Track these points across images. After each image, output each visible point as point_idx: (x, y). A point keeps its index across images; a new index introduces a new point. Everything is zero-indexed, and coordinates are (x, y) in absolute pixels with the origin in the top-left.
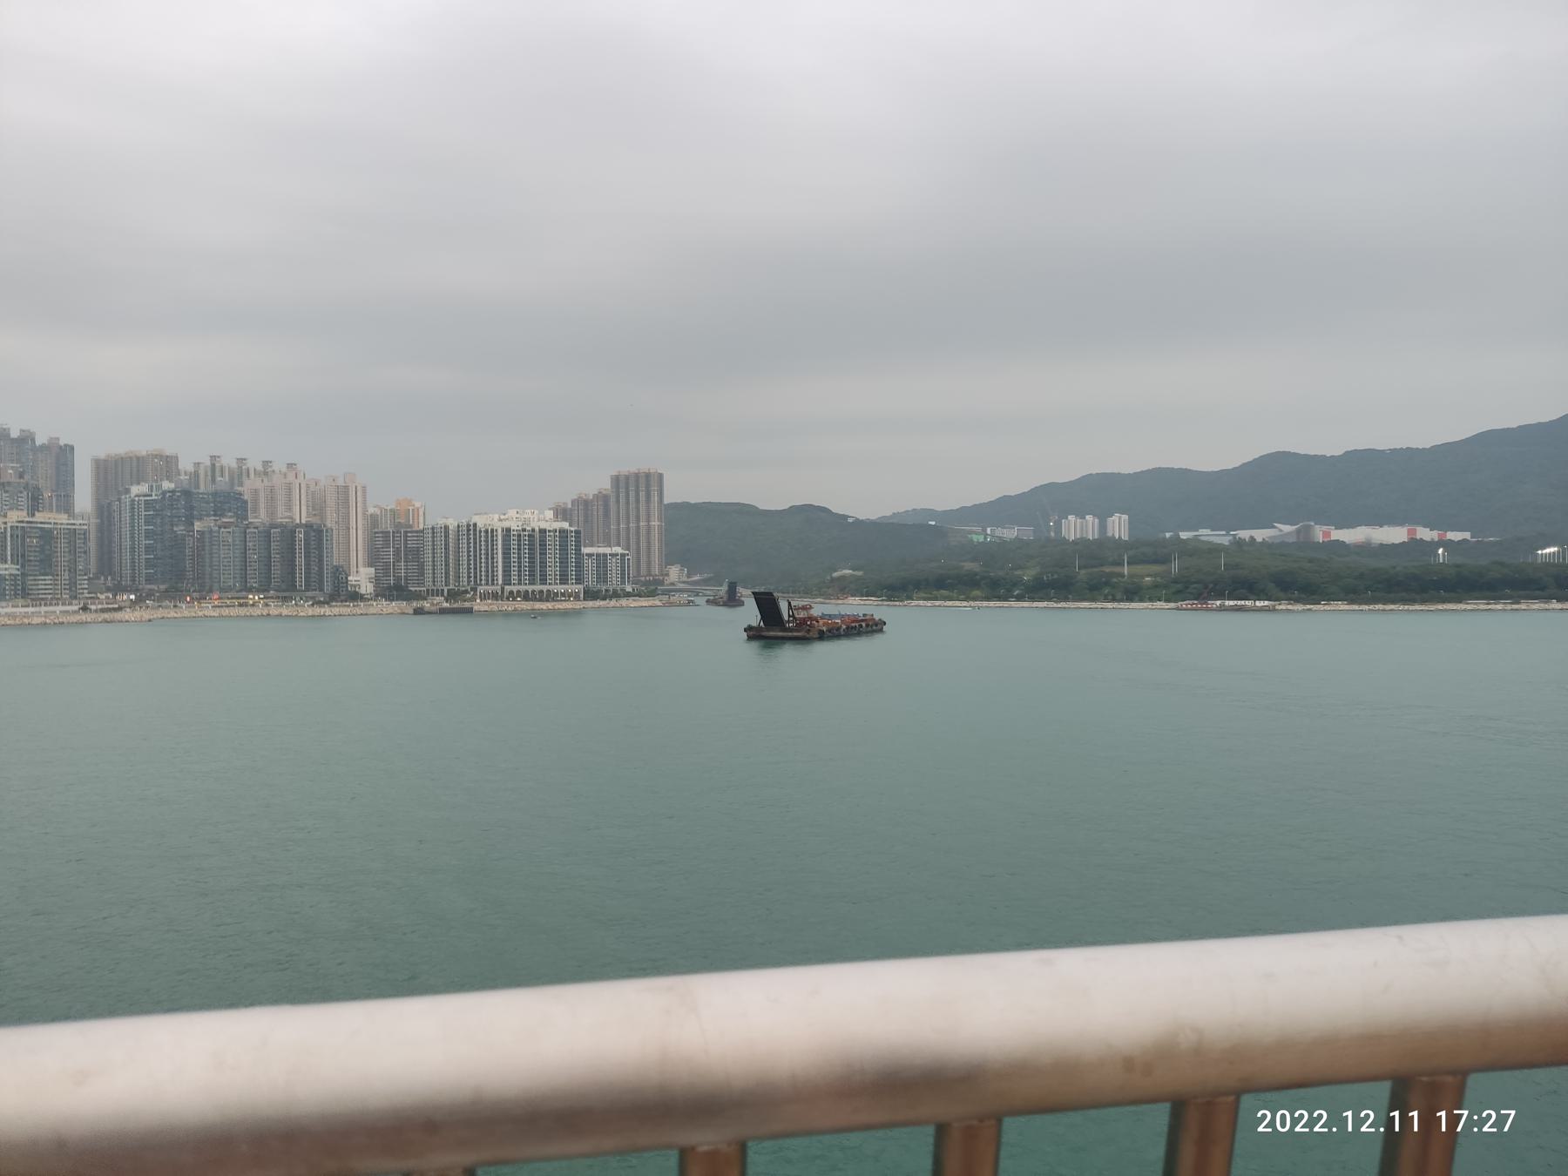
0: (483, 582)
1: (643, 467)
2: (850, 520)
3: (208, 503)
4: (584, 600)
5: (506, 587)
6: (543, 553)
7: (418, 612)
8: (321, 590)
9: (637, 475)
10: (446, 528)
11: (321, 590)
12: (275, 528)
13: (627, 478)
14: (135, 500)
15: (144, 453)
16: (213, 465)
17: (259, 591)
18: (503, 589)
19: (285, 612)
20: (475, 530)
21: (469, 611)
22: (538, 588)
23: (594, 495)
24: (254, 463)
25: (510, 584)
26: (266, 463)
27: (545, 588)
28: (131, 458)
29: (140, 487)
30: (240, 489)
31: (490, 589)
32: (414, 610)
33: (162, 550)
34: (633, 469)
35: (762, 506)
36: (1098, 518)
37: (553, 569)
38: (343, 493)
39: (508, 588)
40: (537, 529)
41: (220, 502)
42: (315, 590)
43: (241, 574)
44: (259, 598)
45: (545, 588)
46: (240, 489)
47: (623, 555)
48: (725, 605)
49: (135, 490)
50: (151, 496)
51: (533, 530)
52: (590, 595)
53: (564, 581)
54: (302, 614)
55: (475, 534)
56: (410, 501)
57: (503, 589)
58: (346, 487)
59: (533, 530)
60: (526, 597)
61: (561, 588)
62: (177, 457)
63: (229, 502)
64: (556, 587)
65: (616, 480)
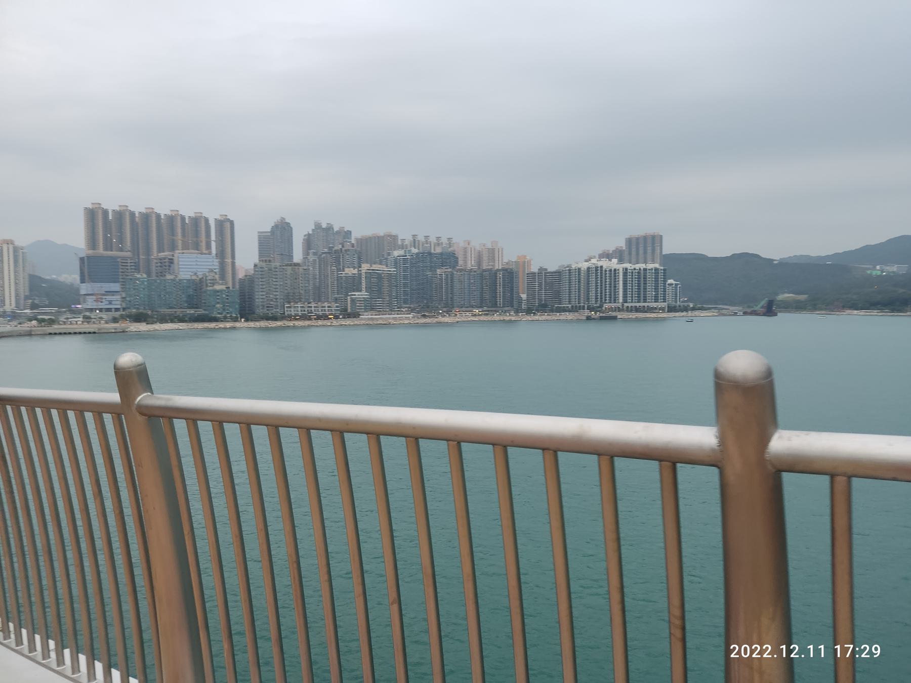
2: (775, 262)
3: (438, 259)
4: (668, 312)
5: (625, 304)
6: (645, 284)
8: (513, 306)
9: (645, 238)
11: (513, 306)
12: (485, 272)
13: (638, 239)
14: (397, 259)
15: (382, 234)
16: (414, 240)
17: (477, 307)
18: (623, 305)
19: (507, 318)
20: (601, 270)
21: (615, 318)
22: (642, 304)
23: (613, 251)
24: (433, 239)
25: (626, 302)
26: (438, 238)
27: (646, 304)
28: (375, 237)
29: (398, 251)
30: (451, 249)
31: (613, 305)
32: (587, 317)
33: (416, 286)
35: (710, 255)
37: (651, 293)
38: (492, 252)
39: (626, 305)
40: (642, 269)
41: (445, 259)
44: (479, 311)
45: (646, 304)
46: (451, 249)
47: (676, 285)
48: (764, 315)
49: (396, 253)
50: (406, 256)
51: (640, 269)
52: (671, 309)
53: (656, 301)
54: (523, 319)
55: (601, 273)
56: (525, 256)
57: (623, 305)
58: (493, 249)
59: (640, 269)
60: (637, 310)
61: (654, 305)
62: (397, 236)
63: (449, 258)
64: (652, 304)
65: (629, 241)
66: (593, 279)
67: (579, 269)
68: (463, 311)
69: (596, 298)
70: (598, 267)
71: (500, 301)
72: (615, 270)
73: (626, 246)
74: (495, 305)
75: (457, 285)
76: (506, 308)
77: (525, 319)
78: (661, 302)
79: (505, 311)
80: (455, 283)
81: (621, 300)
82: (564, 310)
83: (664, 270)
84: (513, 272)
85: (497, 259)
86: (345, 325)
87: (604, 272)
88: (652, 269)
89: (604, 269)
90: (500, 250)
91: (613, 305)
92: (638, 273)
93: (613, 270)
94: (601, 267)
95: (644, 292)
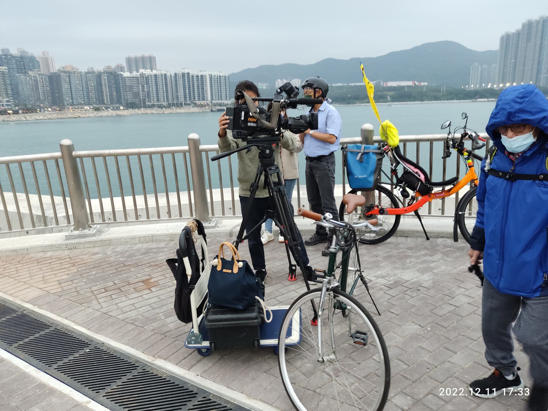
0: (196, 99)
1: (147, 54)
5: (213, 101)
6: (220, 87)
7: (212, 111)
9: (143, 58)
10: (165, 75)
12: (89, 74)
13: (136, 59)
17: (85, 104)
18: (211, 102)
31: (202, 102)
34: (139, 54)
36: (279, 79)
39: (213, 102)
42: (116, 104)
45: (222, 102)
57: (211, 102)
67: (165, 75)
68: (76, 108)
69: (185, 97)
70: (184, 74)
71: (106, 98)
72: (202, 76)
73: (126, 63)
74: (102, 102)
75: (65, 87)
76: (117, 105)
77: (168, 112)
79: (117, 108)
81: (209, 98)
84: (118, 75)
85: (52, 67)
86: (41, 120)
87: (191, 77)
89: (191, 75)
90: (53, 59)
93: (199, 76)
94: (188, 74)
95: (200, 95)
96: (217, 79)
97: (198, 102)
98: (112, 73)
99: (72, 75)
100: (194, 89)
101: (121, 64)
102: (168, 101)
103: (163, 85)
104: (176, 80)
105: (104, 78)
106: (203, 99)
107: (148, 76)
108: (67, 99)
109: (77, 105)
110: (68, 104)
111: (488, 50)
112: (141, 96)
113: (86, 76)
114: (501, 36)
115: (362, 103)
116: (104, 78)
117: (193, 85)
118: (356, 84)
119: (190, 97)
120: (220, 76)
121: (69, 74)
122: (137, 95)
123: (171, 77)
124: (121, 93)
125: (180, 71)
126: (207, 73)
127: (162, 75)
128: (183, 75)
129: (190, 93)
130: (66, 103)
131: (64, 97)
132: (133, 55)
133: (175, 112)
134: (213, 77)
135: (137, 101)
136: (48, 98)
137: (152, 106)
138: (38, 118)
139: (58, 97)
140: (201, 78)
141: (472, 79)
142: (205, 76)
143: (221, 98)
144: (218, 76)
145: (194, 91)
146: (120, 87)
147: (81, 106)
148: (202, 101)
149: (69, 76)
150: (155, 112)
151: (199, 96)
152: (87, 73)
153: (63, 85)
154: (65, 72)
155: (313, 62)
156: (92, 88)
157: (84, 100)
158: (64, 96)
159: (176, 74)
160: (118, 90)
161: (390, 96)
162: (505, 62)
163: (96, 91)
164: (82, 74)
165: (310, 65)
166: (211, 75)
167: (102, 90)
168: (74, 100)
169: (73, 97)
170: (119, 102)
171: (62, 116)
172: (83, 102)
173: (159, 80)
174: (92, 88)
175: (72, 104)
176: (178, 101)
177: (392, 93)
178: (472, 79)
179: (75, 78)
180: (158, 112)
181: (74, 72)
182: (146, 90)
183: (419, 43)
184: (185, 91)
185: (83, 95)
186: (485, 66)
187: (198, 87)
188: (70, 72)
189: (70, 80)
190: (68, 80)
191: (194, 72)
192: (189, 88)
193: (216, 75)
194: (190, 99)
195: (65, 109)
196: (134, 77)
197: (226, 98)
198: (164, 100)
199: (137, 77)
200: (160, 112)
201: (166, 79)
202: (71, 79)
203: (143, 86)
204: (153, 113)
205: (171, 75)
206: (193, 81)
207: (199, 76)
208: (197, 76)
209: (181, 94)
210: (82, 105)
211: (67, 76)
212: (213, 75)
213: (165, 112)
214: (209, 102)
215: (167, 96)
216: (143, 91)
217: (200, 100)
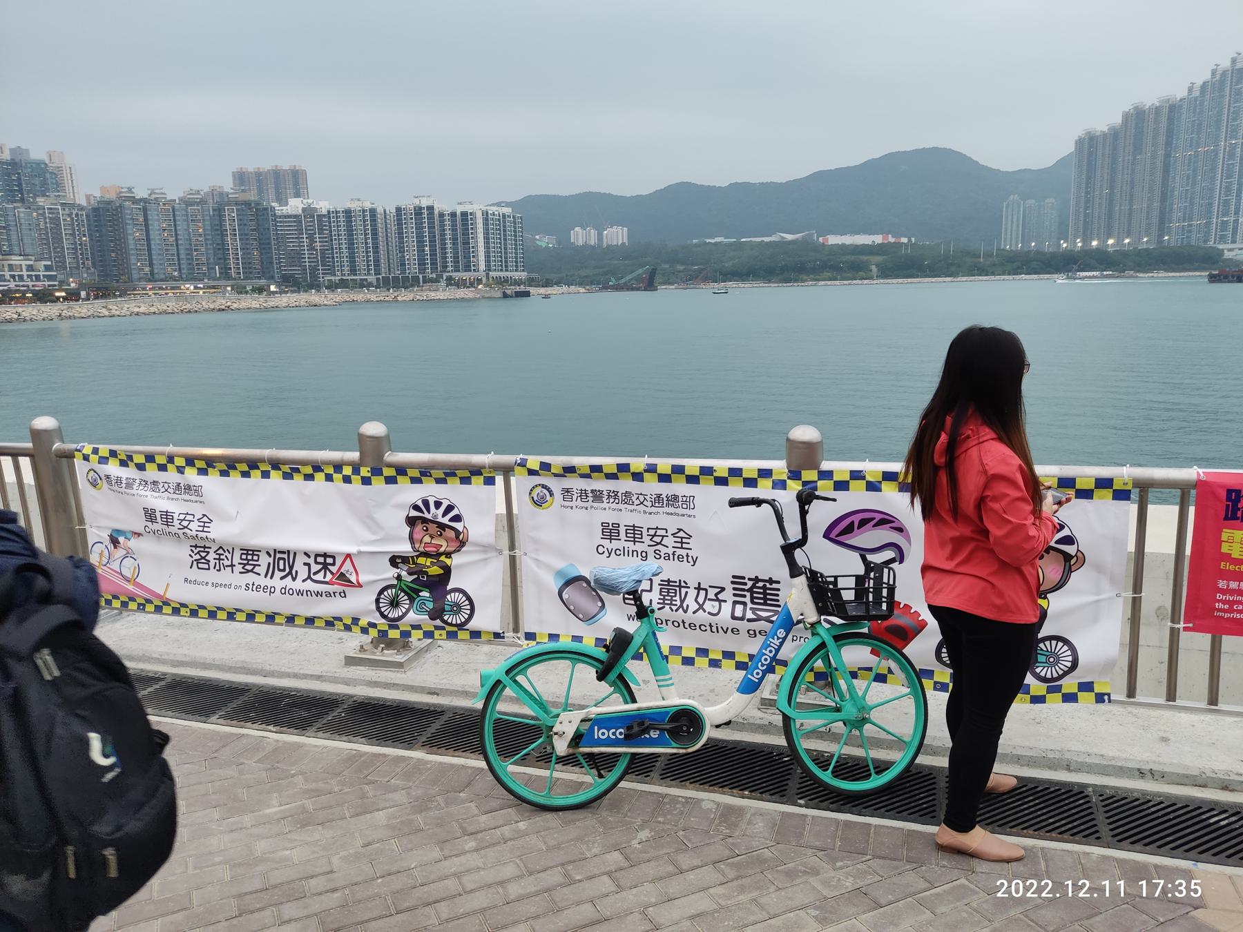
0: (450, 269)
5: (490, 273)
7: (505, 296)
11: (272, 278)
12: (192, 205)
13: (259, 175)
18: (488, 275)
25: (491, 271)
31: (465, 275)
34: (266, 166)
42: (259, 278)
43: (188, 259)
44: (196, 288)
45: (509, 274)
57: (488, 275)
59: (499, 216)
66: (410, 228)
68: (161, 288)
69: (422, 263)
70: (421, 208)
72: (464, 214)
74: (226, 274)
75: (134, 234)
76: (263, 282)
77: (404, 298)
78: (520, 271)
80: (128, 227)
81: (482, 267)
82: (363, 285)
83: (521, 218)
84: (266, 209)
86: (144, 314)
88: (509, 216)
89: (436, 212)
91: (465, 275)
92: (499, 220)
94: (430, 208)
96: (499, 220)
97: (457, 276)
98: (250, 204)
99: (152, 207)
100: (443, 244)
101: (220, 187)
102: (377, 273)
103: (366, 234)
104: (400, 224)
105: (231, 214)
106: (467, 268)
107: (329, 212)
108: (137, 264)
109: (162, 280)
110: (140, 279)
111: (1023, 168)
112: (307, 260)
113: (187, 212)
114: (1077, 138)
115: (819, 280)
116: (231, 214)
117: (443, 235)
118: (767, 239)
119: (434, 263)
120: (504, 215)
121: (145, 205)
122: (296, 257)
123: (385, 217)
124: (272, 253)
125: (409, 203)
126: (476, 208)
127: (364, 211)
128: (418, 211)
129: (433, 254)
130: (135, 276)
131: (133, 259)
132: (250, 167)
133: (425, 298)
134: (490, 216)
135: (296, 271)
136: (83, 263)
137: (343, 284)
138: (137, 310)
139: (115, 261)
140: (462, 220)
141: (1006, 230)
142: (471, 214)
143: (506, 266)
144: (501, 215)
145: (444, 249)
146: (269, 239)
147: (174, 284)
148: (464, 274)
149: (145, 210)
150: (373, 297)
151: (456, 258)
152: (188, 203)
153: (129, 232)
154: (135, 201)
155: (646, 190)
156: (200, 239)
157: (180, 269)
158: (132, 257)
159: (398, 210)
160: (264, 246)
161: (877, 266)
162: (1087, 193)
163: (209, 247)
164: (177, 206)
165: (639, 198)
166: (487, 213)
167: (223, 244)
168: (155, 267)
169: (154, 262)
170: (266, 273)
171: (188, 306)
172: (176, 274)
173: (358, 224)
174: (200, 239)
175: (152, 278)
176: (403, 271)
177: (879, 259)
178: (1006, 230)
179: (158, 215)
180: (382, 299)
181: (156, 199)
182: (318, 245)
183: (877, 154)
184: (421, 250)
185: (178, 255)
186: (1031, 202)
187: (455, 239)
188: (145, 201)
189: (146, 220)
190: (141, 219)
191: (444, 205)
192: (432, 241)
193: (496, 213)
194: (434, 269)
195: (135, 289)
196: (289, 216)
197: (517, 266)
198: (369, 270)
199: (295, 216)
200: (387, 298)
201: (375, 221)
202: (150, 217)
203: (311, 238)
204: (368, 301)
205: (385, 211)
206: (442, 226)
207: (458, 213)
208: (453, 215)
209: (411, 255)
210: (175, 280)
211: (140, 209)
212: (490, 212)
213: (399, 298)
214: (481, 274)
215: (377, 261)
216: (311, 248)
217: (459, 271)
